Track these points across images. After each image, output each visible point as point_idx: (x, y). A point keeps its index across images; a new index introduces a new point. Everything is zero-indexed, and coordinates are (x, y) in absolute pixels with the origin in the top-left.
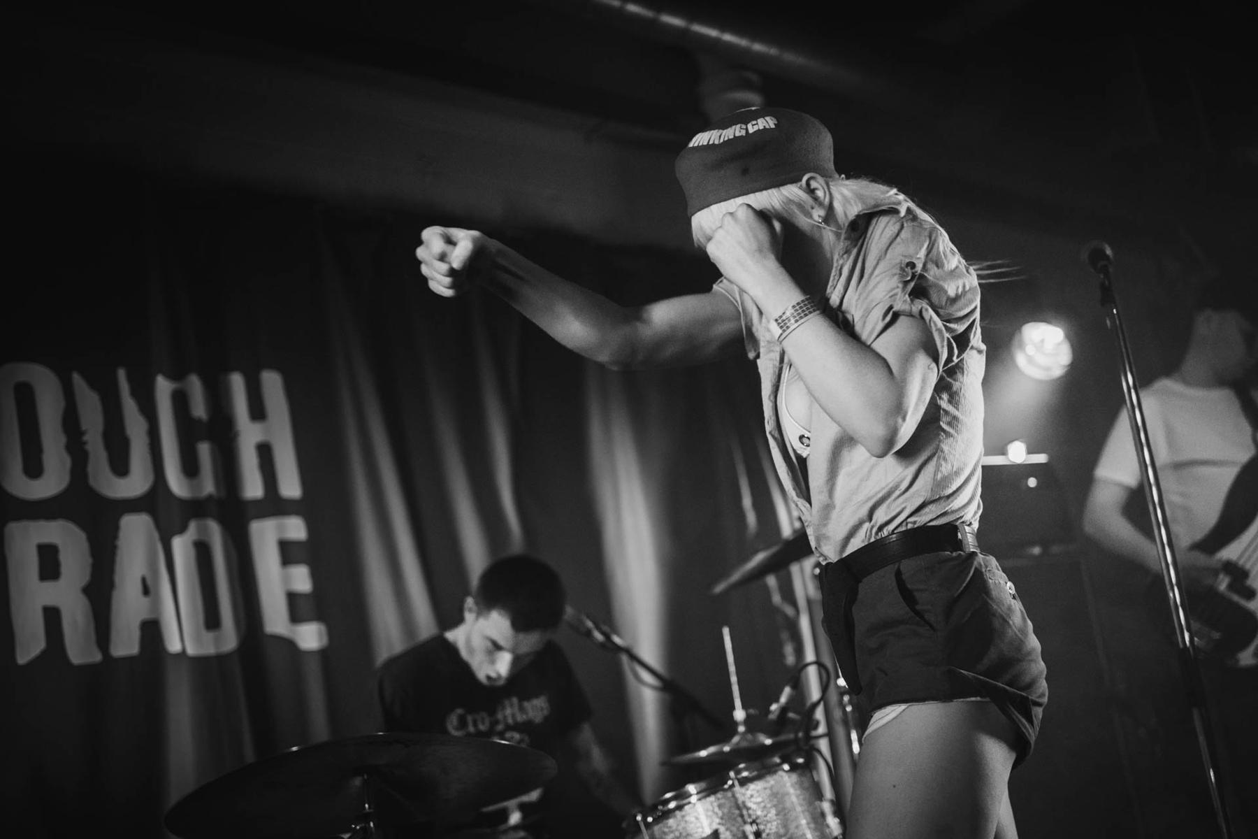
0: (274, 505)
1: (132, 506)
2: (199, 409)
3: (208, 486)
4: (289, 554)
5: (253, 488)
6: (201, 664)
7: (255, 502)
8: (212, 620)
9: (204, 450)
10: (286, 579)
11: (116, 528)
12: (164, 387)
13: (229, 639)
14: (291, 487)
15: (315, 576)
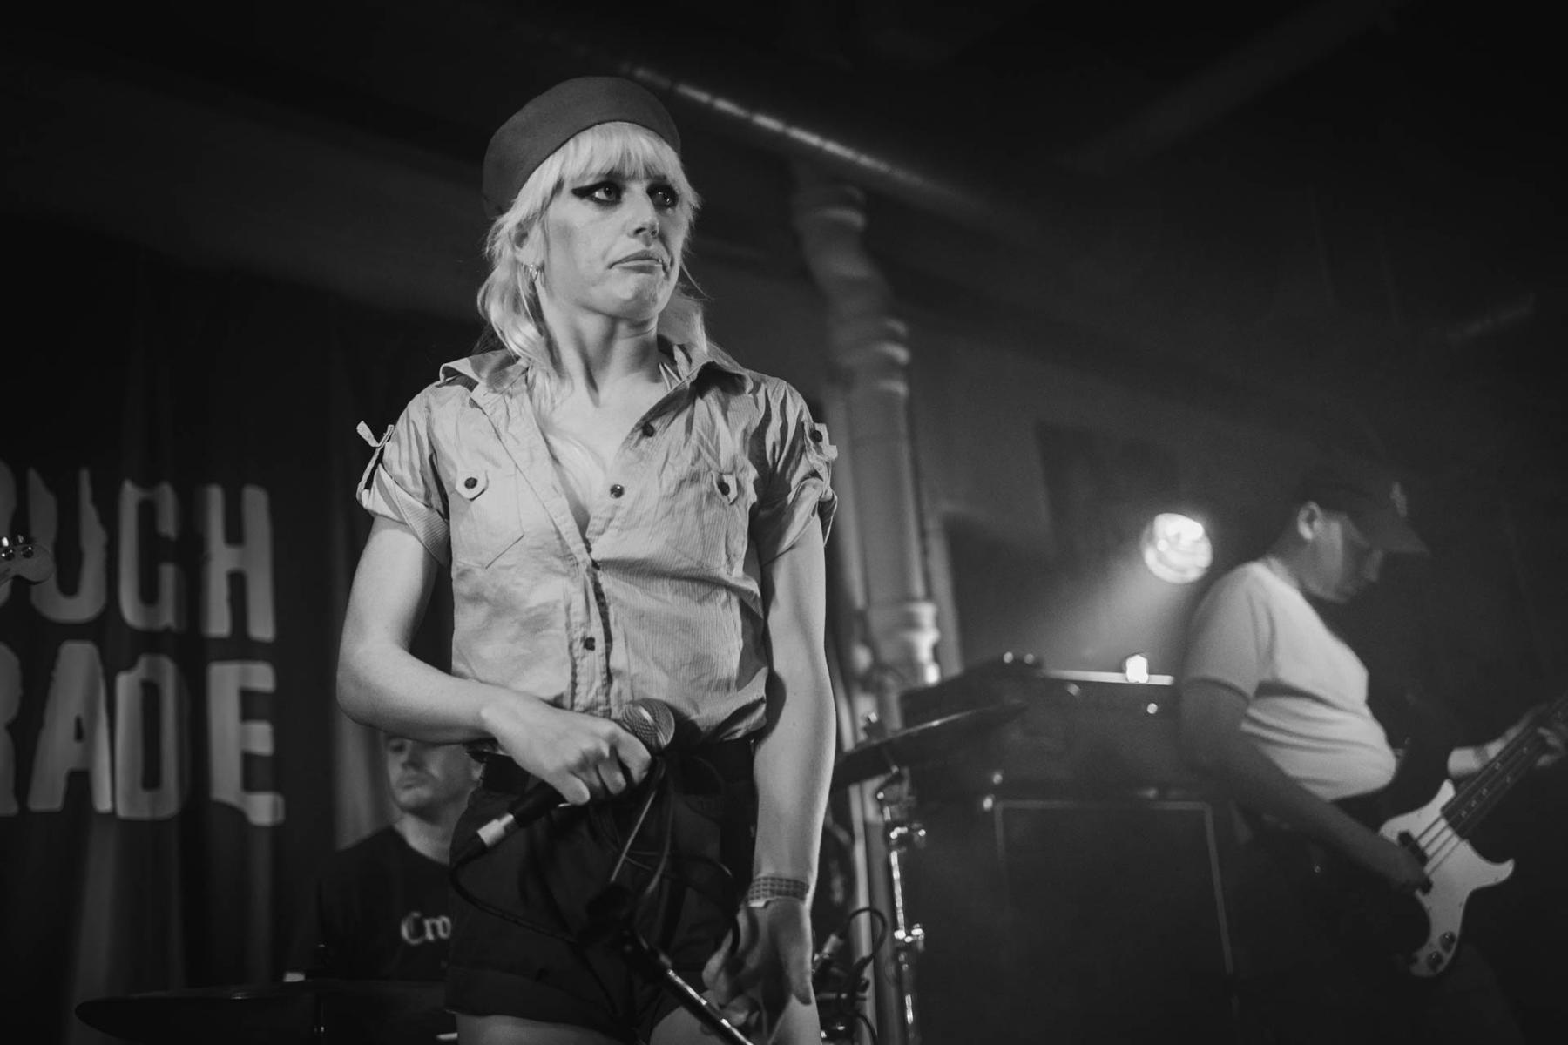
0: (240, 647)
1: (77, 631)
2: (168, 525)
3: (167, 616)
4: (251, 705)
5: (219, 624)
6: (129, 825)
7: (219, 641)
8: (151, 778)
9: (168, 574)
10: (244, 737)
11: (54, 656)
12: (130, 495)
13: (170, 802)
14: (262, 627)
15: (278, 737)
